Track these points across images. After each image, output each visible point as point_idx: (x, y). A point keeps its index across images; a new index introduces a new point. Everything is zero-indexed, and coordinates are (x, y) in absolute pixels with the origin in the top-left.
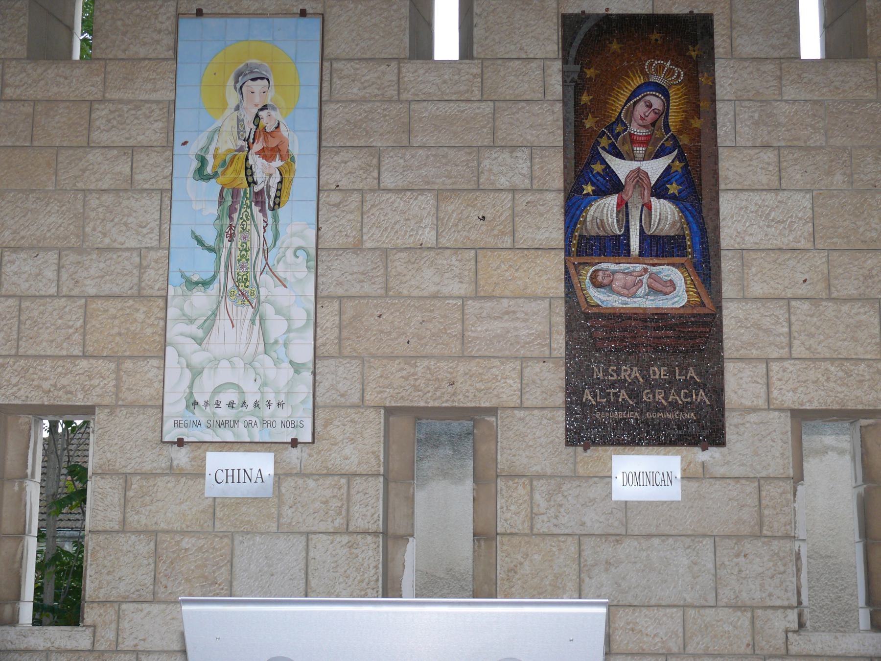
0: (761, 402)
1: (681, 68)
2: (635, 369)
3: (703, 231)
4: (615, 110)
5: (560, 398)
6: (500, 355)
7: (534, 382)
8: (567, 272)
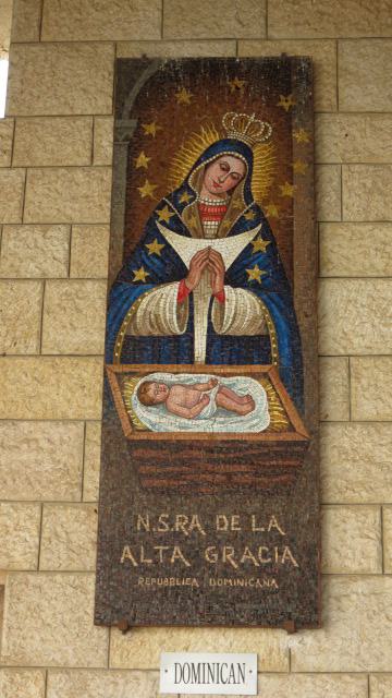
0: (374, 567)
1: (269, 123)
2: (195, 517)
3: (294, 330)
4: (181, 175)
5: (90, 559)
6: (12, 498)
7: (57, 535)
8: (106, 385)
